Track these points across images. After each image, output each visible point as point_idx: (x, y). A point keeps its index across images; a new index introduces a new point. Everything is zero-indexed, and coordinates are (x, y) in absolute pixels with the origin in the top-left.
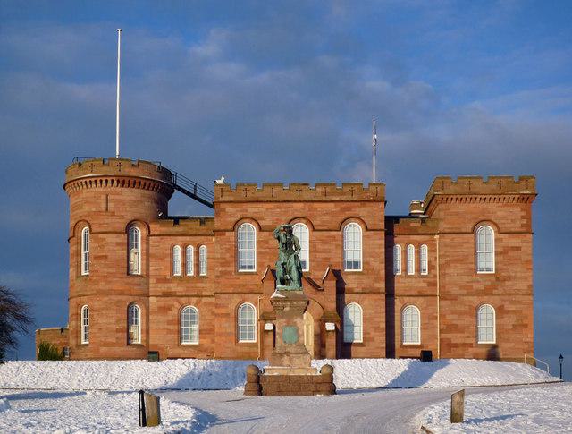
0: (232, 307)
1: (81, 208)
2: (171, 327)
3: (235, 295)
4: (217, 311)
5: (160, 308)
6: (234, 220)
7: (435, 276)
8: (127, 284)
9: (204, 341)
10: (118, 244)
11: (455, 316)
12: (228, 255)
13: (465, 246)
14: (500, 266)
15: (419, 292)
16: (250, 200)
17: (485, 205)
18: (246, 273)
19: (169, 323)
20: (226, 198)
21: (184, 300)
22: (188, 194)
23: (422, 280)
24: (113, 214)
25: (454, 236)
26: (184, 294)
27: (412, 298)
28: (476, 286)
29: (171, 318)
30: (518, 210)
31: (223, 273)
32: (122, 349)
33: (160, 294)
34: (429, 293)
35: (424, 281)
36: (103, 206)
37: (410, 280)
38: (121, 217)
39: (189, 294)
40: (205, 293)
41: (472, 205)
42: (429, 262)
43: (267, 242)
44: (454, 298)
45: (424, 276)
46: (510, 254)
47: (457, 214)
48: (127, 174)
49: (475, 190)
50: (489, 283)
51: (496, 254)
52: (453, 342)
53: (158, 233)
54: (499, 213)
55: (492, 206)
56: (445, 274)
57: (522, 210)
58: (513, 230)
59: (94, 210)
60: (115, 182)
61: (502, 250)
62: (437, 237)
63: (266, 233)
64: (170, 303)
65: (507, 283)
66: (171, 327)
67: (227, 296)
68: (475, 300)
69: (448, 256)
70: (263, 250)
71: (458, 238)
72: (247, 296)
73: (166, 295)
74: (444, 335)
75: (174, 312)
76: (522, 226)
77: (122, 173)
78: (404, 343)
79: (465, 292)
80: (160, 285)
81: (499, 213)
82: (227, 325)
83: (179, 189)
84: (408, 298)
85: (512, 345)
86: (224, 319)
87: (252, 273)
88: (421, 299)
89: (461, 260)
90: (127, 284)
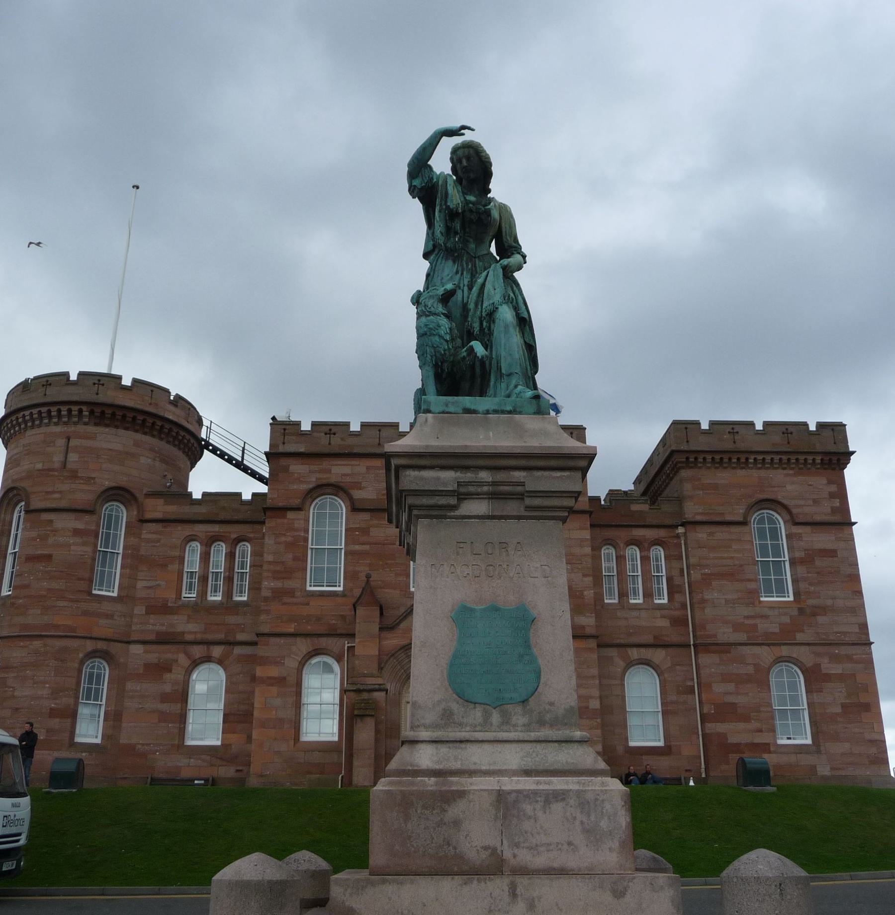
0: (291, 663)
1: (18, 465)
2: (164, 707)
3: (298, 639)
4: (260, 672)
5: (147, 666)
6: (305, 487)
7: (684, 606)
8: (85, 613)
9: (233, 738)
10: (77, 532)
11: (731, 687)
12: (290, 556)
13: (735, 547)
14: (803, 586)
15: (655, 637)
16: (337, 450)
17: (763, 473)
18: (322, 594)
19: (165, 698)
20: (291, 448)
21: (197, 651)
22: (230, 460)
23: (658, 613)
24: (74, 475)
25: (713, 529)
26: (199, 637)
27: (643, 650)
28: (763, 626)
29: (168, 688)
30: (820, 482)
31: (278, 595)
32: (56, 754)
33: (152, 637)
34: (675, 638)
35: (663, 617)
36: (58, 459)
37: (635, 613)
38: (90, 480)
39: (210, 637)
40: (241, 637)
41: (741, 473)
42: (669, 580)
43: (365, 531)
44: (724, 648)
45: (661, 607)
46: (819, 562)
47: (715, 487)
48: (109, 400)
49: (742, 446)
50: (787, 620)
51: (793, 562)
52: (732, 740)
53: (159, 515)
54: (789, 487)
55: (778, 476)
56: (703, 601)
57: (830, 482)
58: (818, 518)
59: (39, 466)
60: (86, 413)
61: (802, 554)
62: (681, 530)
63: (365, 516)
64: (169, 656)
65: (821, 619)
66: (164, 707)
67: (281, 641)
68: (765, 654)
69: (707, 566)
70: (358, 547)
71: (721, 534)
72: (324, 642)
73: (165, 640)
74: (711, 727)
75: (177, 674)
76: (834, 510)
77: (101, 398)
78: (632, 744)
79: (742, 637)
80: (153, 619)
81: (789, 487)
82: (278, 702)
83: (214, 450)
84: (635, 650)
85: (847, 745)
86: (274, 690)
87: (334, 594)
88: (658, 656)
89: (730, 575)
90: (85, 613)
